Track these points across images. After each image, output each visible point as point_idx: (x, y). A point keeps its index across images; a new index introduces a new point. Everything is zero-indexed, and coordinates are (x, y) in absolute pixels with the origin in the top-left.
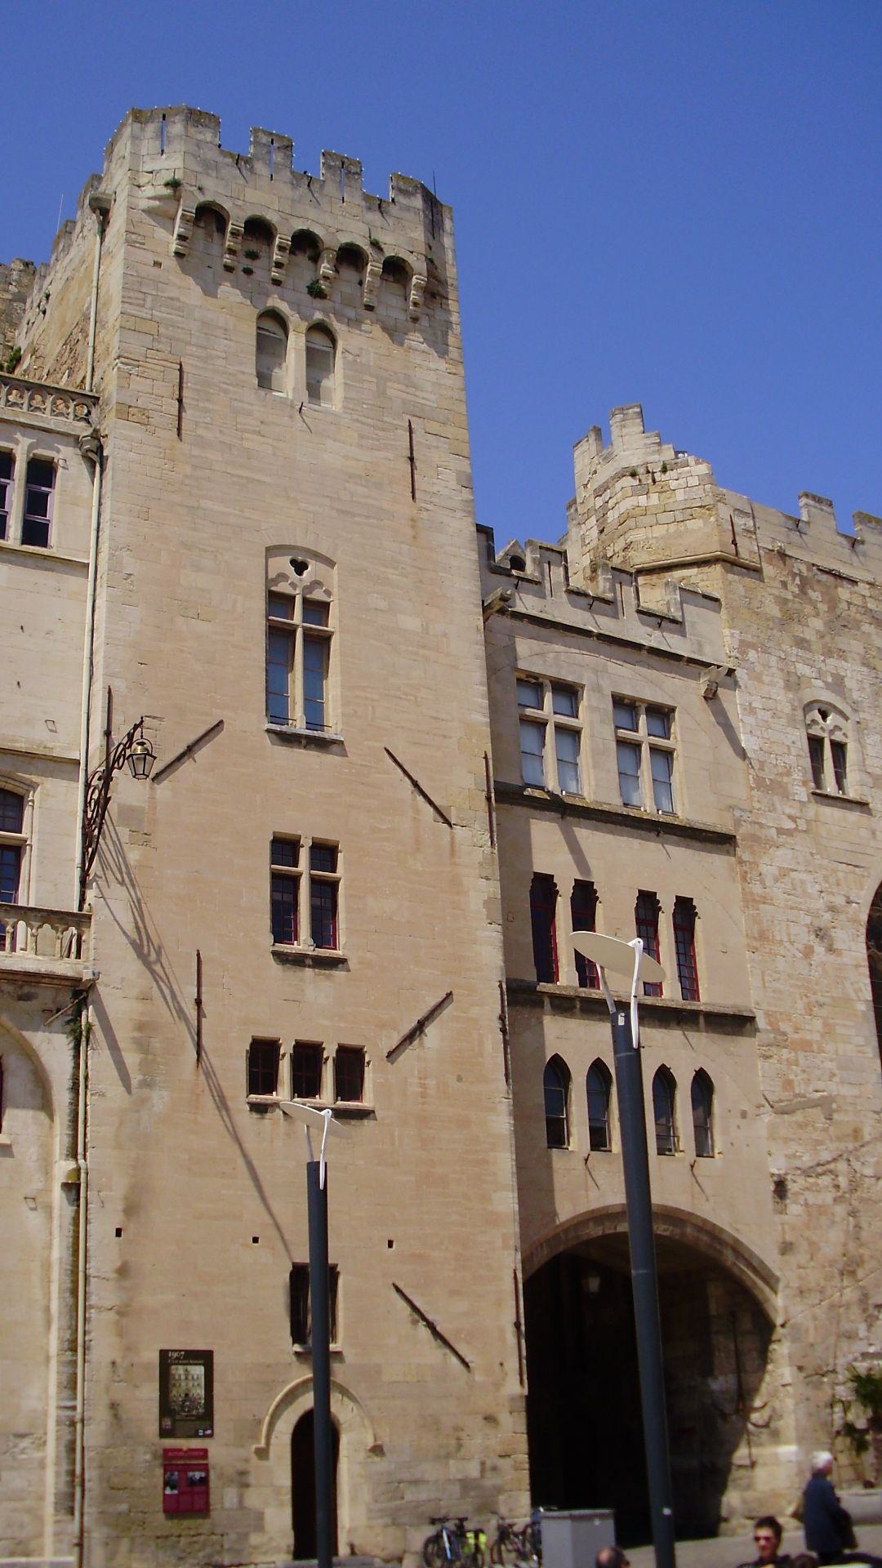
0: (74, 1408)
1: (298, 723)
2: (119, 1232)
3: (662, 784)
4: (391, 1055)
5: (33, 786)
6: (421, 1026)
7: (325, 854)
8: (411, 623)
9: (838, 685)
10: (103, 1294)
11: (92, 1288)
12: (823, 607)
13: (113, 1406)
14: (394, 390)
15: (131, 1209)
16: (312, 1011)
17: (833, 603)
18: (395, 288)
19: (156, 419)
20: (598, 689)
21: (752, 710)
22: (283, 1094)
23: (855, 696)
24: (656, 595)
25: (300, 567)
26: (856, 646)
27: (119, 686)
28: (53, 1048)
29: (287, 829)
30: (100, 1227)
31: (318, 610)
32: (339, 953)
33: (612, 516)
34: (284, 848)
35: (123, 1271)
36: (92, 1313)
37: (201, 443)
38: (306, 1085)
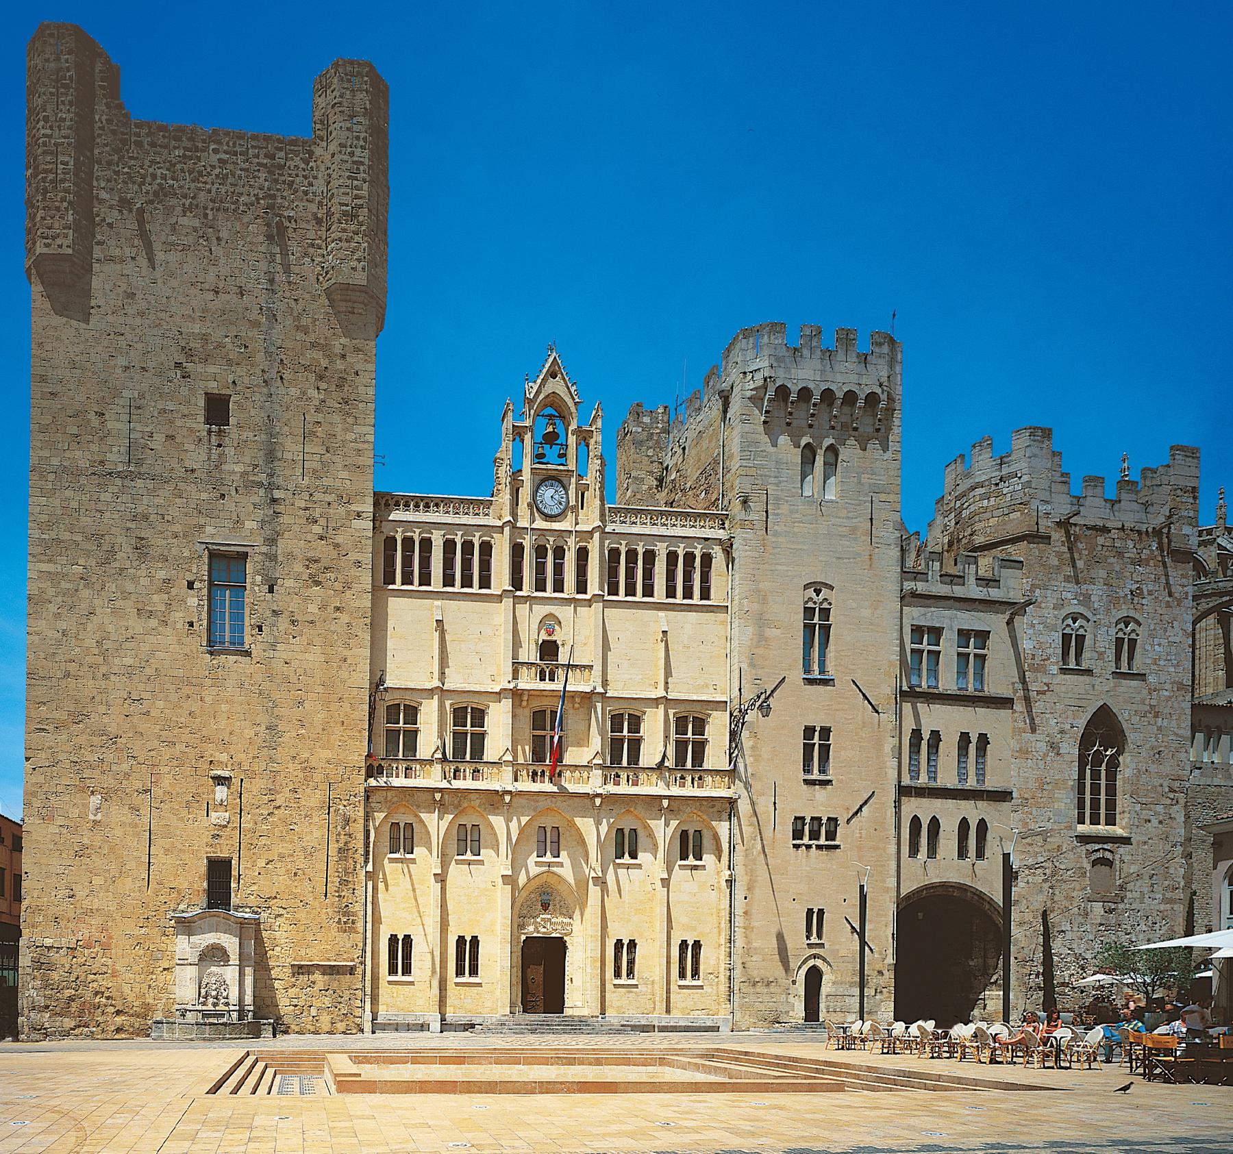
1: (816, 674)
3: (980, 676)
4: (848, 821)
5: (709, 715)
6: (860, 809)
7: (826, 732)
16: (819, 804)
20: (951, 629)
21: (1033, 626)
22: (806, 840)
24: (985, 563)
25: (818, 592)
27: (744, 666)
28: (723, 828)
31: (825, 613)
32: (828, 778)
33: (965, 513)
34: (809, 731)
37: (776, 534)
38: (815, 835)
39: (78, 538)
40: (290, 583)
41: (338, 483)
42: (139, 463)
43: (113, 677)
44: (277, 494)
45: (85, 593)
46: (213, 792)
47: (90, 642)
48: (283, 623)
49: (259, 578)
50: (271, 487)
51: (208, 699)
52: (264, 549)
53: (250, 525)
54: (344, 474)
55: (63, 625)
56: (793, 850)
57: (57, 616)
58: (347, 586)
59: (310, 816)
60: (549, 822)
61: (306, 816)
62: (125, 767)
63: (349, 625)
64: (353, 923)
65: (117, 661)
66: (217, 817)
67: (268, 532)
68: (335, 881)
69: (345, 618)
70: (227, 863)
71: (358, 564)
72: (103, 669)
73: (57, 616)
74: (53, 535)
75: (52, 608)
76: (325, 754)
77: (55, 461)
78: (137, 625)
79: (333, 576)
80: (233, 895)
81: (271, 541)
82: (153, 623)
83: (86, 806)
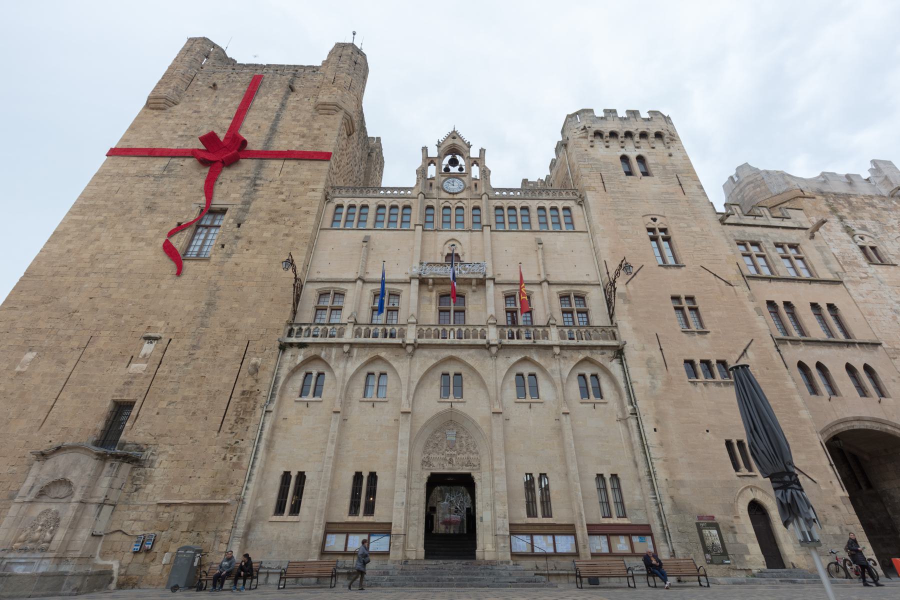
0: (656, 498)
2: (655, 430)
6: (745, 351)
8: (697, 229)
9: (864, 228)
10: (655, 453)
11: (651, 451)
12: (847, 205)
13: (672, 497)
14: (668, 168)
15: (657, 422)
17: (850, 204)
18: (660, 141)
19: (598, 189)
23: (874, 230)
25: (655, 220)
26: (866, 215)
27: (607, 260)
29: (676, 294)
30: (648, 428)
34: (676, 298)
35: (661, 444)
36: (653, 461)
39: (109, 203)
40: (254, 222)
41: (302, 177)
42: (172, 171)
43: (92, 275)
44: (258, 182)
45: (98, 230)
46: (141, 348)
47: (86, 255)
48: (240, 243)
49: (231, 220)
50: (256, 178)
51: (164, 287)
52: (240, 206)
53: (233, 195)
54: (309, 173)
55: (70, 246)
56: (691, 386)
57: (69, 242)
58: (296, 223)
59: (223, 366)
60: (452, 369)
61: (220, 365)
62: (71, 332)
63: (293, 243)
64: (239, 458)
65: (101, 266)
66: (138, 367)
67: (246, 198)
68: (231, 417)
69: (291, 239)
70: (130, 405)
71: (307, 212)
72: (88, 270)
73: (69, 242)
74: (92, 202)
75: (69, 238)
76: (251, 320)
77: (115, 171)
78: (127, 244)
79: (286, 219)
80: (123, 433)
81: (247, 203)
82: (142, 244)
83: (18, 361)
